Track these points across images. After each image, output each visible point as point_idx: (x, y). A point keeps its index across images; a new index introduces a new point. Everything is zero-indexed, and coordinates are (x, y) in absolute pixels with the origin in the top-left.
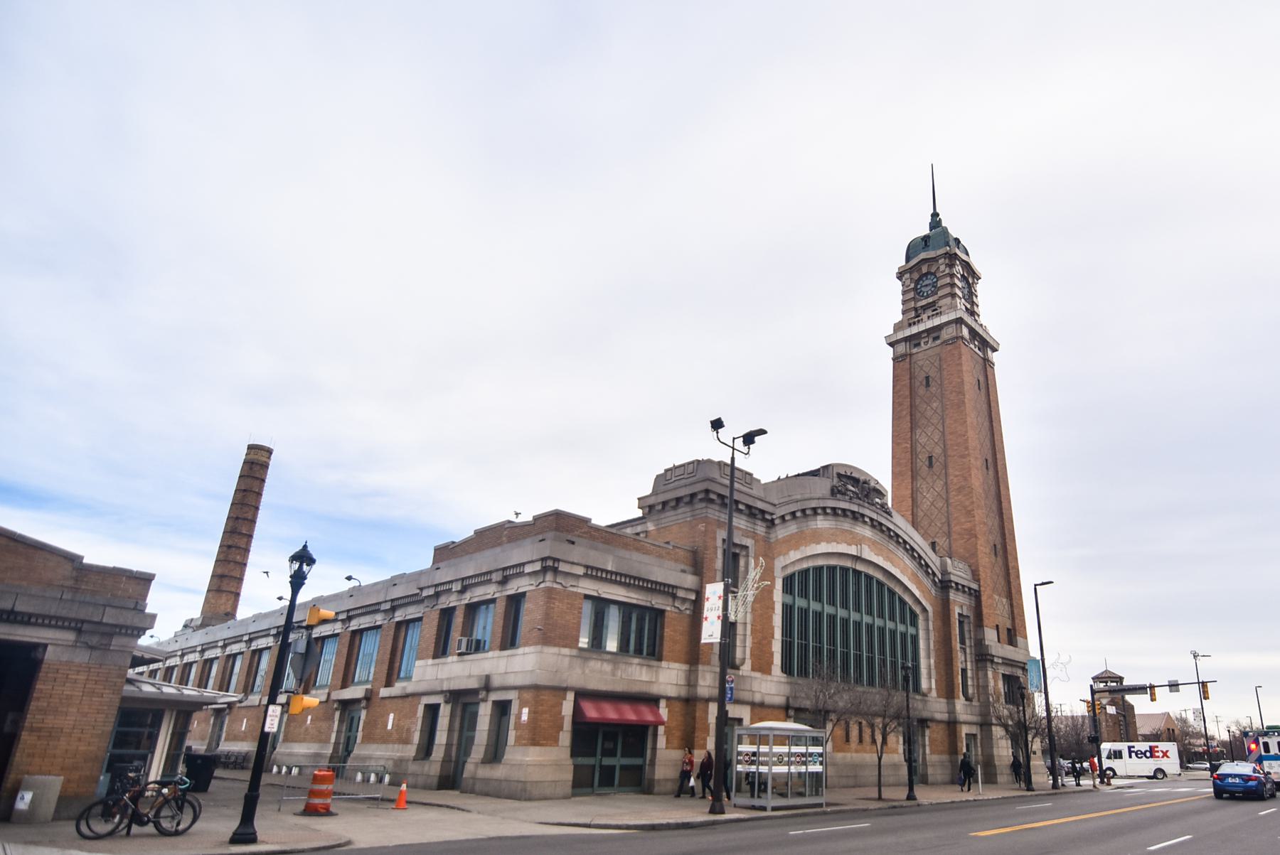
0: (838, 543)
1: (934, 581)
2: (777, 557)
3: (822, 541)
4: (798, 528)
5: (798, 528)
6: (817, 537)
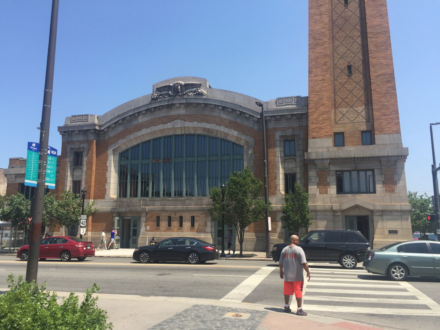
0: (155, 126)
1: (254, 121)
2: (109, 146)
3: (143, 128)
4: (124, 128)
5: (124, 128)
6: (139, 128)
